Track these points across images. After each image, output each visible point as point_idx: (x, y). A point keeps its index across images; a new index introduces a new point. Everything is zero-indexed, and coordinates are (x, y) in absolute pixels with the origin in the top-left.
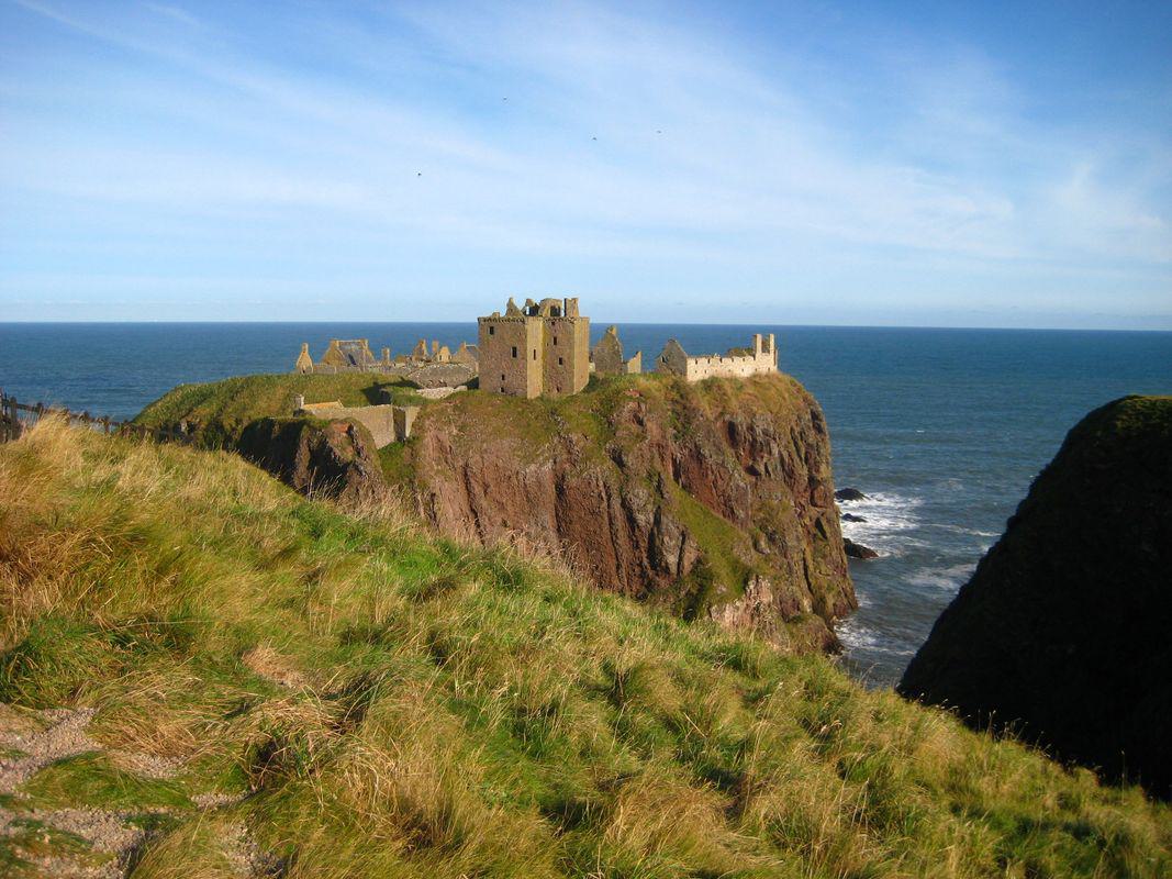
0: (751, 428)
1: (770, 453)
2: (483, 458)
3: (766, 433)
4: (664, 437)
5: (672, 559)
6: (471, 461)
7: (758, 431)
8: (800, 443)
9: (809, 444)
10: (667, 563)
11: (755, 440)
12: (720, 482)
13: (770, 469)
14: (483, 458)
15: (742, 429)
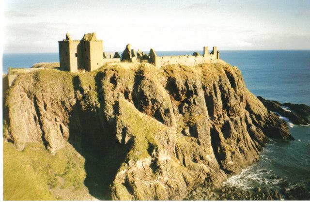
0: (186, 84)
1: (196, 94)
2: (43, 95)
3: (194, 86)
4: (127, 88)
5: (120, 138)
6: (37, 96)
7: (190, 85)
8: (218, 90)
9: (223, 91)
10: (118, 141)
11: (188, 88)
12: (156, 107)
13: (196, 102)
14: (43, 95)
15: (180, 83)
